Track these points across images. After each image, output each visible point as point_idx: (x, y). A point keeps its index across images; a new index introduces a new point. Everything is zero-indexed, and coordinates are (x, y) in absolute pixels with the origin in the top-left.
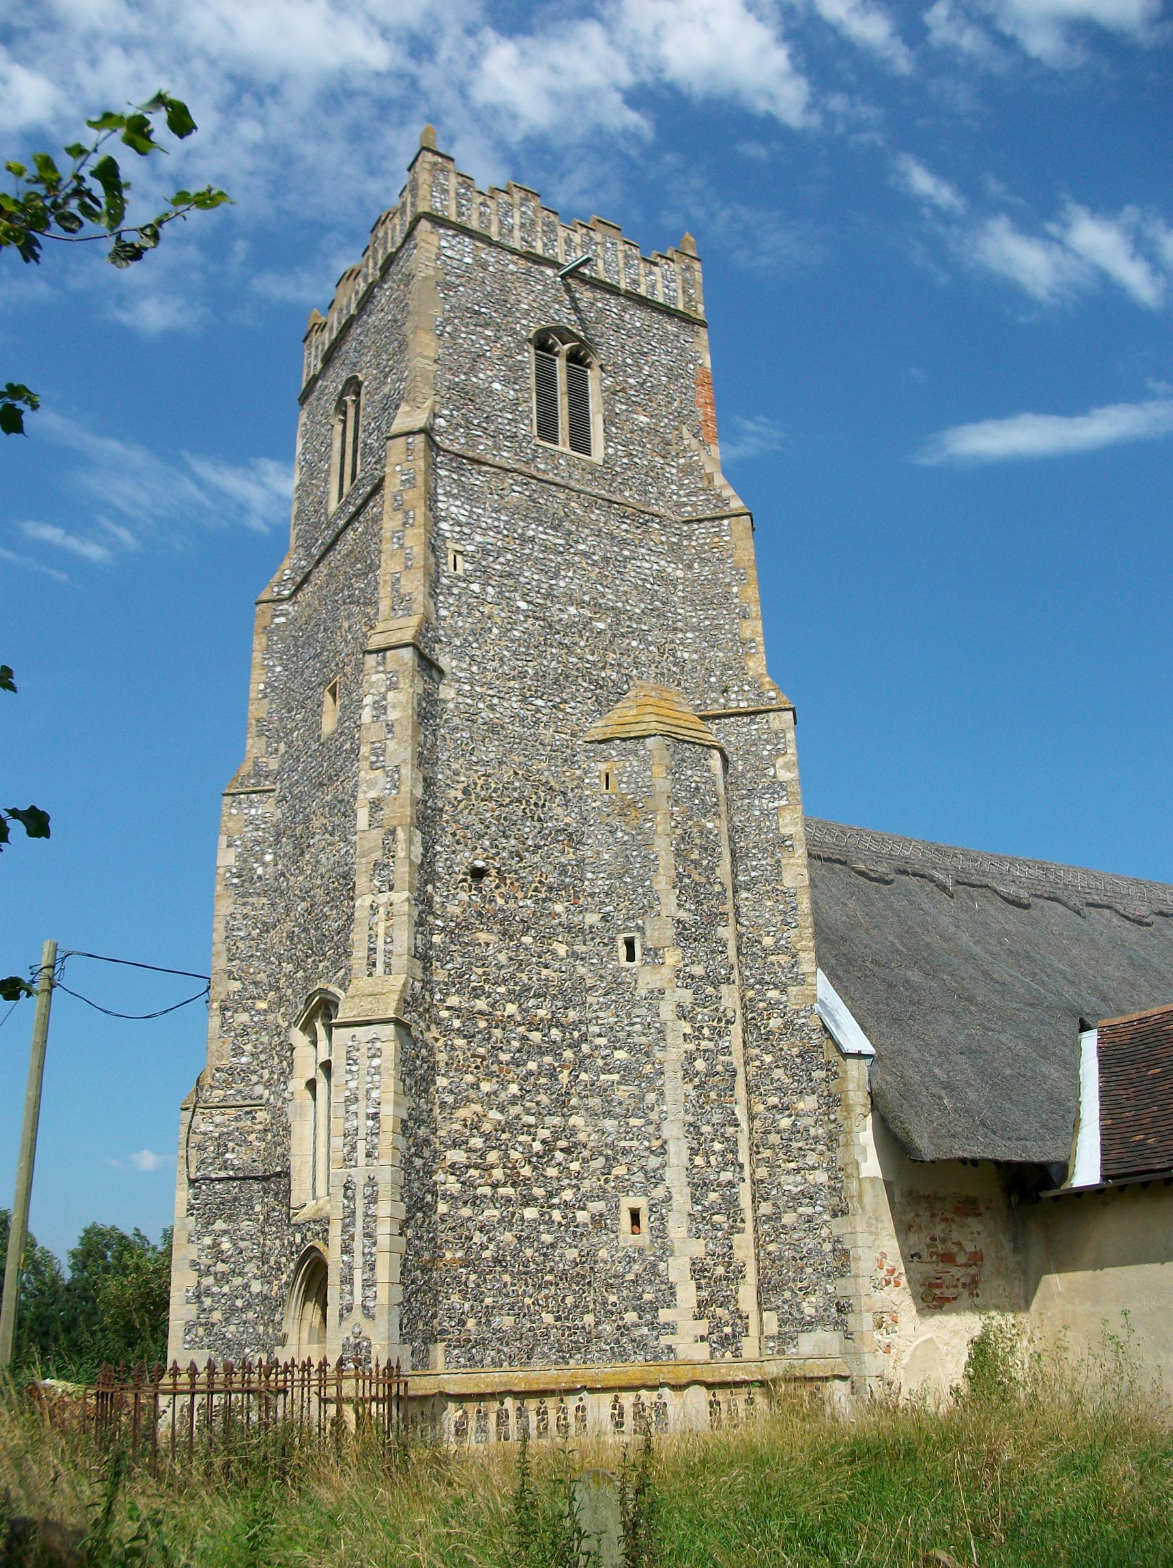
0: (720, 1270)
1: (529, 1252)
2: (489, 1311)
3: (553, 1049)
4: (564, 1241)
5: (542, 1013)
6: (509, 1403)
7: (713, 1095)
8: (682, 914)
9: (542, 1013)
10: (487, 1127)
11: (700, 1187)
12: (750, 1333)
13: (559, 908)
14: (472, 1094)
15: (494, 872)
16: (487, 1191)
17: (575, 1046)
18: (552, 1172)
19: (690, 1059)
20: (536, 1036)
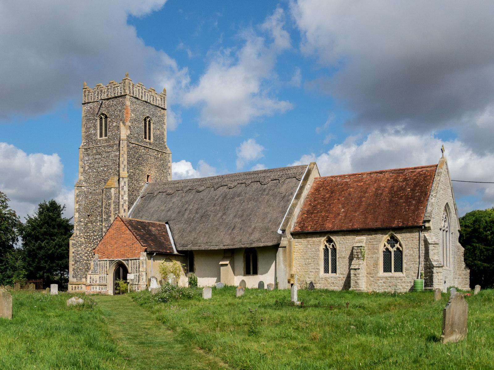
16: (90, 259)
20: (95, 237)
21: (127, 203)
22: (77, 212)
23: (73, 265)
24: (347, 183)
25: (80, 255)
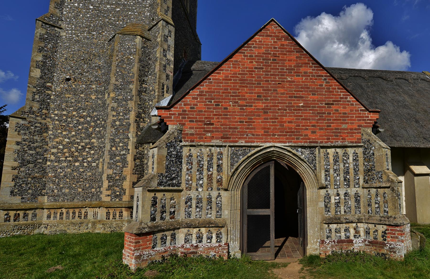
0: (118, 177)
1: (75, 174)
2: (61, 188)
3: (88, 123)
4: (87, 171)
5: (84, 114)
6: (64, 210)
7: (121, 131)
8: (117, 83)
9: (84, 114)
10: (64, 143)
11: (113, 155)
12: (126, 194)
13: (94, 86)
14: (60, 135)
15: (72, 79)
16: (64, 159)
17: (95, 122)
18: (85, 154)
19: (114, 121)
20: (82, 120)
23: (14, 168)
25: (38, 150)
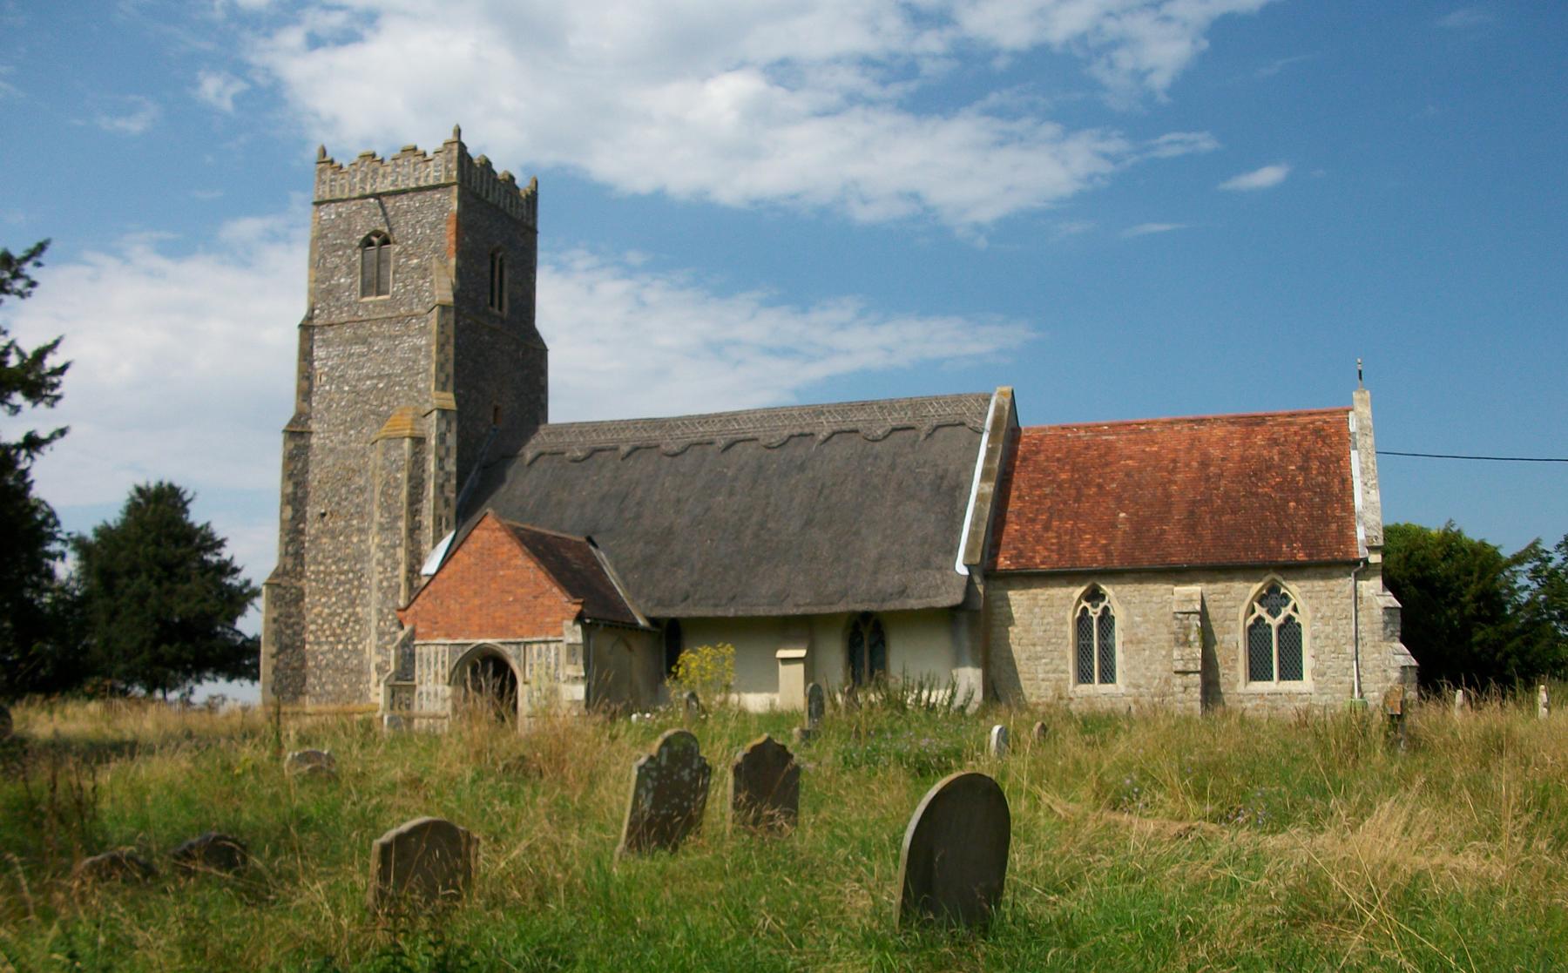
21: (454, 482)
22: (288, 503)
24: (1110, 447)
